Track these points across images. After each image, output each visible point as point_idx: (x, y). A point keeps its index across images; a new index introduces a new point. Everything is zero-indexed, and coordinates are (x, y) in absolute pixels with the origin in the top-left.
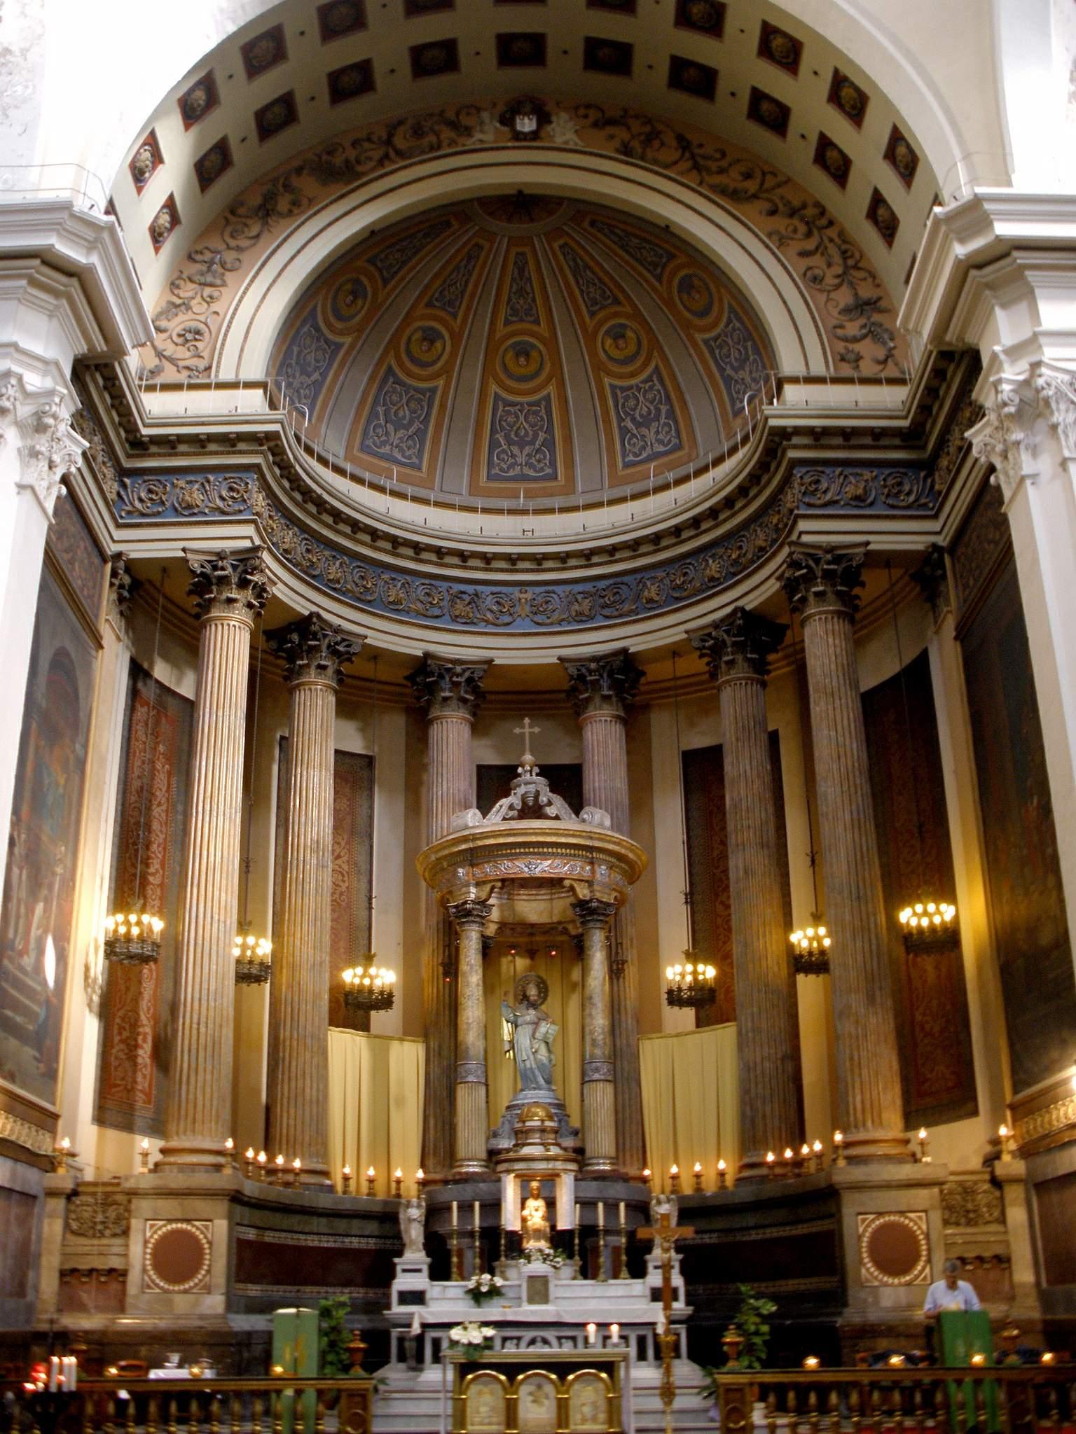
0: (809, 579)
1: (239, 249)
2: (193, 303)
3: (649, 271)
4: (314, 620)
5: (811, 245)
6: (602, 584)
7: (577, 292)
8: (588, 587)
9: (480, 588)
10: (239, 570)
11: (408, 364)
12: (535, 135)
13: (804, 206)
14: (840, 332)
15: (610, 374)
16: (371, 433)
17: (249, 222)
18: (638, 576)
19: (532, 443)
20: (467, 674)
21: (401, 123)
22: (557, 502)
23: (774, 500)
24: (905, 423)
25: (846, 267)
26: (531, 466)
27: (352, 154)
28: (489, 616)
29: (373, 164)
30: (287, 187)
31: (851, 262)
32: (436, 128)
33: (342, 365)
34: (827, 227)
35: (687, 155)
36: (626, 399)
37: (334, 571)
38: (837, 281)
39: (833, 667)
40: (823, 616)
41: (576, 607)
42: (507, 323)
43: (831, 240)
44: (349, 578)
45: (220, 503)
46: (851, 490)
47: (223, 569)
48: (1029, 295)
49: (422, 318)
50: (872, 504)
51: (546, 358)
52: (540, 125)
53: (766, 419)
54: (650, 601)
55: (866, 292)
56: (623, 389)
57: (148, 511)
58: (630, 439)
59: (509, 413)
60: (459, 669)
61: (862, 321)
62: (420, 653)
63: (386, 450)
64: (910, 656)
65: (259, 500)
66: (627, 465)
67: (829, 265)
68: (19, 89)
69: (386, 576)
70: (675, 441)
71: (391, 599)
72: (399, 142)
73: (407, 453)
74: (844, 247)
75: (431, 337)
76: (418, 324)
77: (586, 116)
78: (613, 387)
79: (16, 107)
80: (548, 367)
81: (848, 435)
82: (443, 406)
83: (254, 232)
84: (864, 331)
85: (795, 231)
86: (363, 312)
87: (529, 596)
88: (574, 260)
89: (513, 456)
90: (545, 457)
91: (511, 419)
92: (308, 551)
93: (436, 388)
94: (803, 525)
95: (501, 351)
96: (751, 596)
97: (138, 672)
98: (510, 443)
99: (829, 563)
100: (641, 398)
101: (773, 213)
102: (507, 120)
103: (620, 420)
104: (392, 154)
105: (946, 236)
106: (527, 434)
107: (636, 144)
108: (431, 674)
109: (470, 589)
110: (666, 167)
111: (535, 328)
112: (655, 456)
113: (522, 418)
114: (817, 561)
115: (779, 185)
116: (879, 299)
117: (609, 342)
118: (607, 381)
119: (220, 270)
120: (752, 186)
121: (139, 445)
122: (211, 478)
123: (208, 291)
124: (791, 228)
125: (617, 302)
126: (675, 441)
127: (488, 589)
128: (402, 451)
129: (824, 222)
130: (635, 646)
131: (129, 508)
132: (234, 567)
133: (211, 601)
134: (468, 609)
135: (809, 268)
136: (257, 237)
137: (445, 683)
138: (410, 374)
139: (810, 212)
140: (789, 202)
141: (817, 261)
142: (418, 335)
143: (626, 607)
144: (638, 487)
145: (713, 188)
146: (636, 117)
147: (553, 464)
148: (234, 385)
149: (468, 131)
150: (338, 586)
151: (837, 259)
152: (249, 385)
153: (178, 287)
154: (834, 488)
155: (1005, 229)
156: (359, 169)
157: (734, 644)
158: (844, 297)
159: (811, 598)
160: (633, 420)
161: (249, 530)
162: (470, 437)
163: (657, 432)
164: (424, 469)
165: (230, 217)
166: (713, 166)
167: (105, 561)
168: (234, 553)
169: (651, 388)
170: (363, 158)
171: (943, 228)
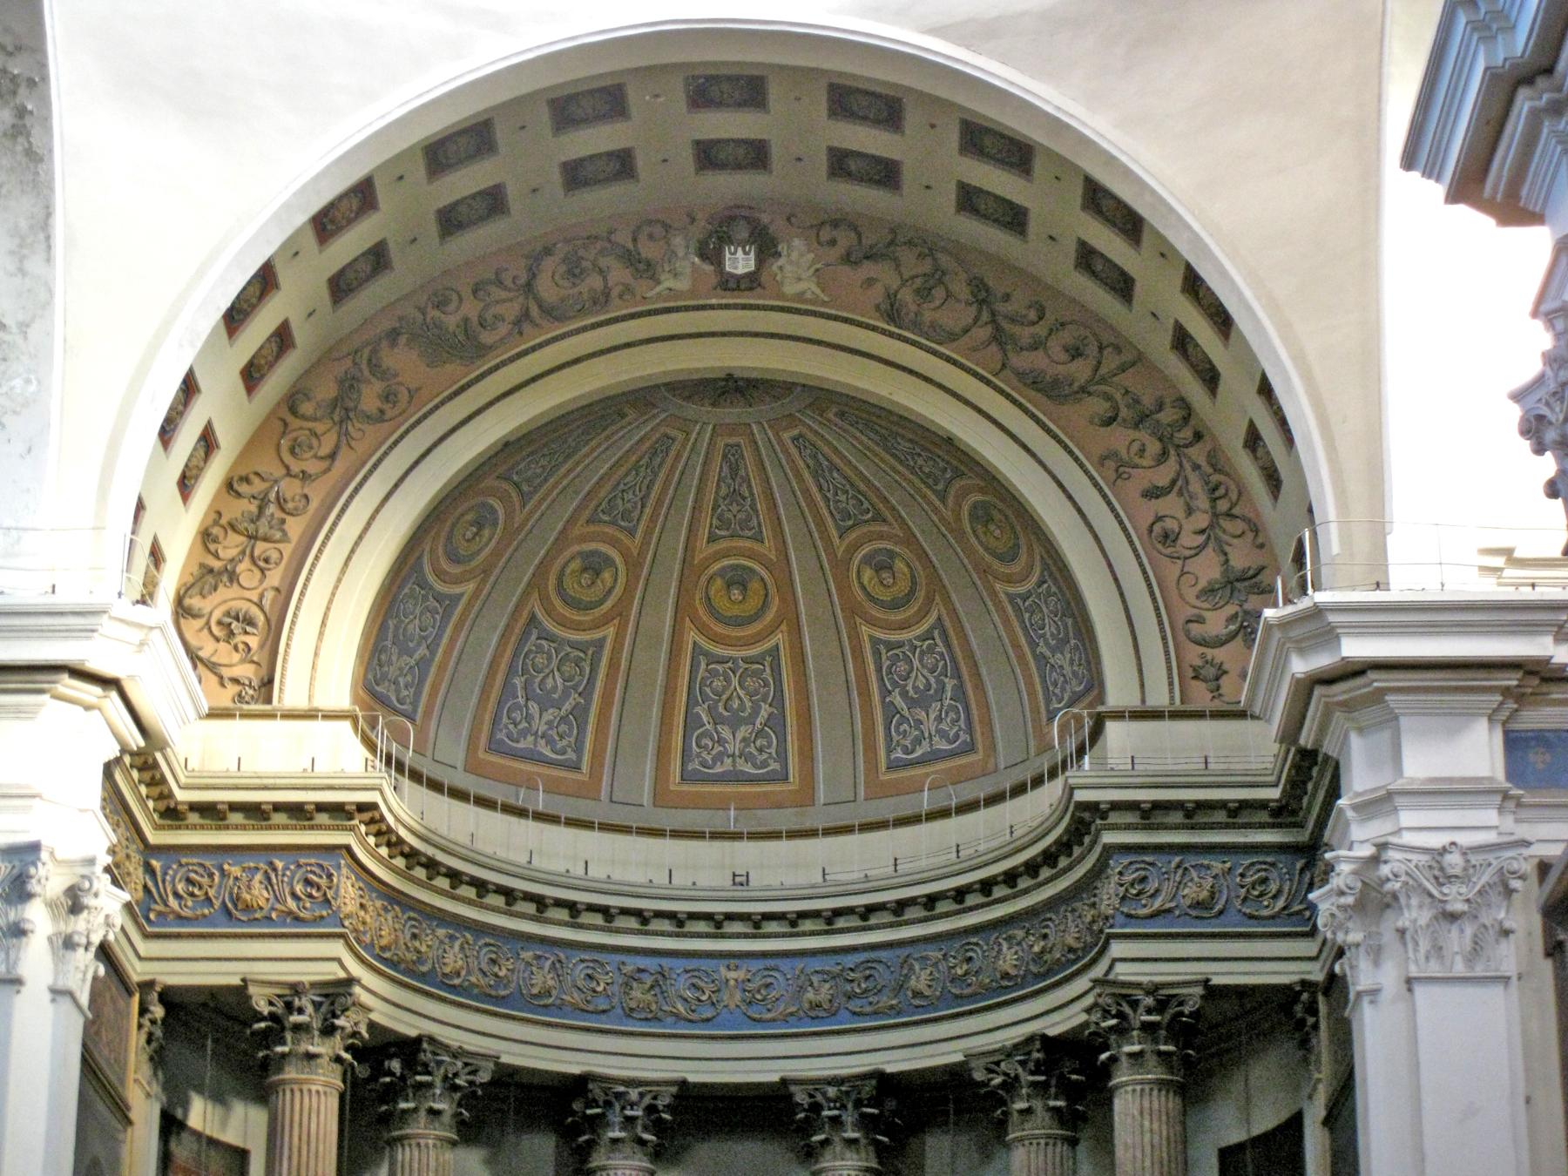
0: (1122, 1031)
1: (305, 476)
2: (241, 568)
3: (929, 487)
4: (425, 1045)
5: (1163, 476)
6: (851, 960)
7: (818, 497)
8: (829, 964)
9: (666, 962)
10: (324, 1009)
11: (558, 603)
12: (751, 282)
13: (1160, 407)
14: (1195, 629)
15: (872, 622)
16: (505, 720)
17: (319, 427)
18: (903, 952)
19: (751, 720)
20: (647, 1100)
21: (548, 251)
22: (785, 819)
23: (1087, 885)
24: (1274, 794)
25: (1216, 515)
26: (748, 758)
27: (471, 309)
28: (681, 1007)
29: (503, 329)
30: (375, 366)
31: (1223, 506)
32: (603, 262)
33: (458, 628)
34: (1190, 445)
35: (985, 316)
36: (895, 660)
37: (453, 959)
38: (1201, 539)
39: (1148, 1163)
40: (1138, 1088)
41: (810, 995)
42: (712, 539)
43: (1196, 467)
44: (474, 964)
45: (292, 904)
46: (1191, 892)
47: (301, 1011)
48: (1391, 720)
49: (583, 539)
50: (1221, 912)
51: (772, 590)
52: (760, 262)
53: (1072, 789)
54: (917, 994)
55: (1241, 558)
56: (890, 646)
57: (187, 913)
58: (899, 724)
59: (714, 673)
60: (634, 1094)
61: (1231, 609)
62: (576, 1070)
63: (526, 743)
64: (1284, 1115)
65: (348, 892)
66: (892, 767)
67: (1190, 511)
68: (18, 382)
69: (527, 955)
70: (964, 737)
71: (535, 991)
72: (547, 289)
73: (560, 745)
74: (1216, 478)
75: (594, 565)
76: (576, 548)
77: (833, 242)
78: (875, 642)
79: (15, 412)
80: (775, 604)
81: (1194, 813)
82: (613, 665)
83: (325, 450)
84: (1232, 627)
85: (1142, 451)
86: (493, 543)
87: (741, 974)
88: (815, 457)
89: (721, 741)
90: (769, 746)
91: (718, 684)
92: (414, 936)
93: (603, 640)
94: (1117, 949)
95: (704, 579)
96: (1056, 1017)
97: (171, 1125)
98: (717, 720)
99: (1149, 1011)
100: (916, 663)
101: (1109, 422)
102: (711, 253)
103: (885, 692)
104: (535, 311)
105: (1281, 645)
106: (742, 707)
107: (906, 296)
108: (593, 1103)
109: (650, 963)
110: (952, 337)
111: (756, 546)
112: (934, 757)
113: (735, 682)
114: (1134, 1004)
115: (1123, 368)
116: (1261, 569)
117: (868, 574)
118: (865, 630)
119: (279, 514)
120: (1080, 370)
121: (172, 814)
122: (280, 865)
123: (260, 547)
124: (1136, 447)
125: (879, 518)
126: (964, 737)
127: (679, 965)
128: (550, 742)
129: (1186, 434)
130: (895, 1064)
131: (160, 908)
132: (317, 1006)
133: (283, 1056)
134: (649, 997)
135: (1159, 519)
136: (332, 456)
137: (615, 1117)
138: (563, 623)
139: (1168, 416)
140: (1137, 401)
141: (1171, 505)
142: (575, 565)
143: (886, 1000)
144: (904, 805)
145: (1021, 375)
146: (910, 243)
147: (782, 756)
148: (310, 715)
149: (646, 269)
150: (456, 981)
151: (1203, 502)
152: (330, 716)
153: (215, 541)
154: (1168, 888)
155: (1356, 648)
156: (487, 338)
157: (1034, 1084)
158: (1208, 569)
159: (1124, 1059)
160: (904, 694)
161: (337, 948)
162: (655, 711)
163: (939, 719)
164: (585, 767)
165: (290, 418)
166: (1025, 334)
167: (130, 993)
168: (314, 985)
169: (931, 649)
170: (489, 316)
171: (1277, 635)
